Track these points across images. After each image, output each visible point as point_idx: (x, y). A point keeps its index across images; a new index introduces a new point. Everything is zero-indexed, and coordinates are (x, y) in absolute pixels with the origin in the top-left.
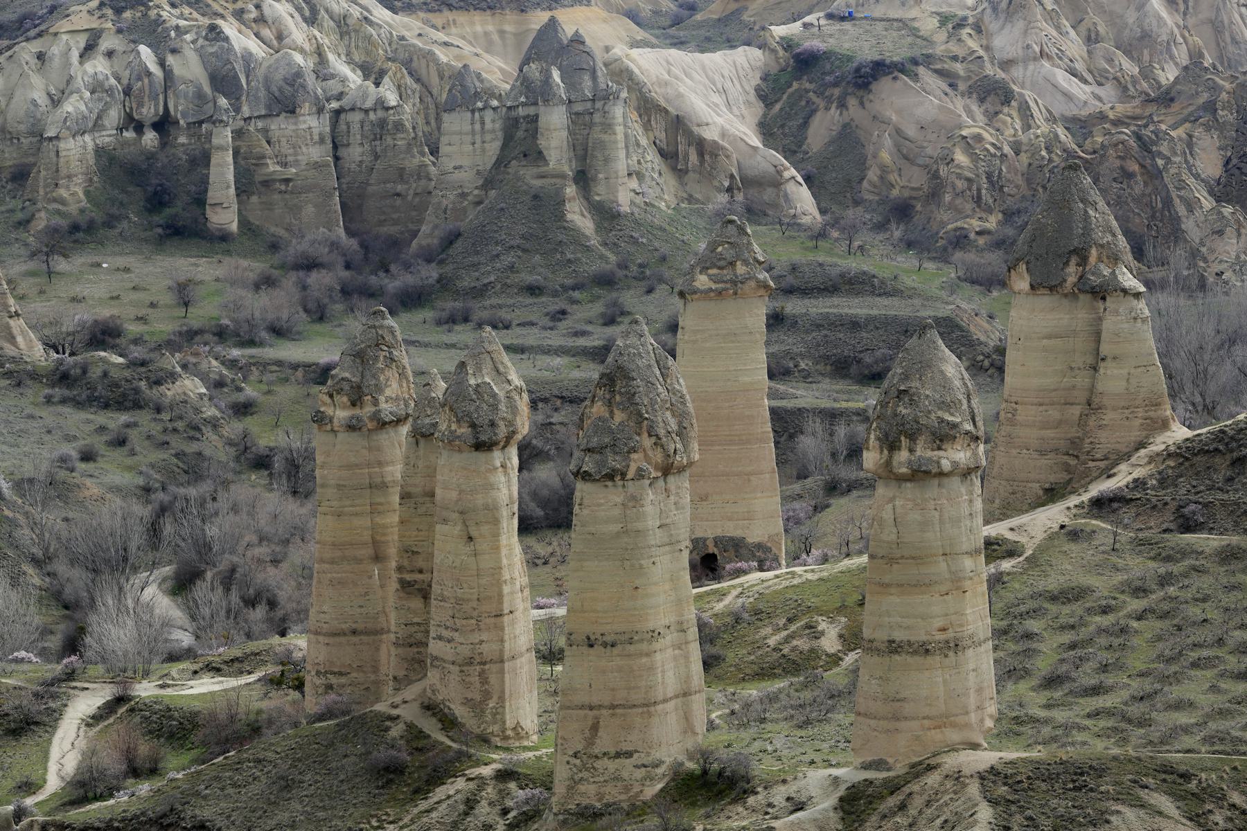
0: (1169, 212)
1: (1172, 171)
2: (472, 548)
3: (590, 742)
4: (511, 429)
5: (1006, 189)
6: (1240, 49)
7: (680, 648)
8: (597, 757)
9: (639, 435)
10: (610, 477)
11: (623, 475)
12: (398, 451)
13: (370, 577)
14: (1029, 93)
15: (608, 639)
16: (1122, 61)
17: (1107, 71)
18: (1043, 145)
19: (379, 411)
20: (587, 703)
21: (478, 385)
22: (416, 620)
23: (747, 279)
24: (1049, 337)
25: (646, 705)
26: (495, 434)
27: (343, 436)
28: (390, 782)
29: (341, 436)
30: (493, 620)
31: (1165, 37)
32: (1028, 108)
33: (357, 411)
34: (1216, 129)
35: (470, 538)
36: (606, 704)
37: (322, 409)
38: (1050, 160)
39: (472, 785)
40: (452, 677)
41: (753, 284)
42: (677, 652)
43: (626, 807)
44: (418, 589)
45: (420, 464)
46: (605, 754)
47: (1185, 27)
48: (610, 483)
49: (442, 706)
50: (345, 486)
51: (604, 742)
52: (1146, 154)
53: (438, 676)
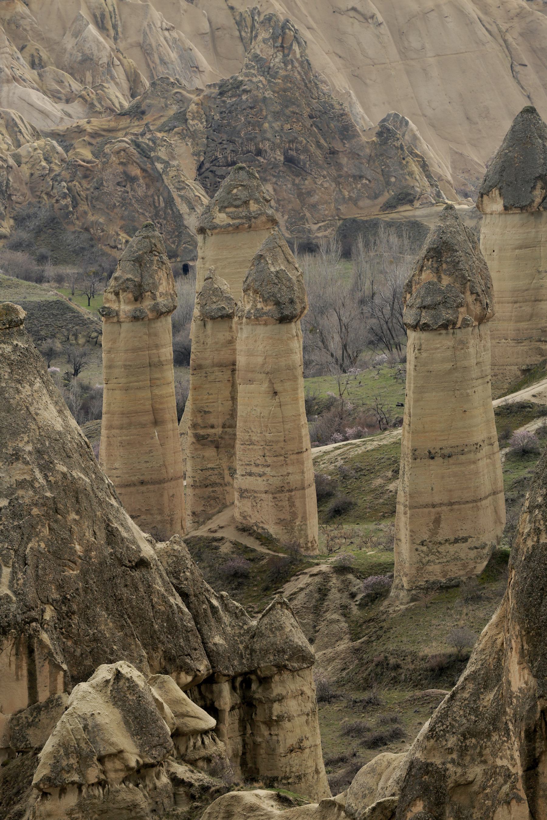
0: (172, 210)
1: (172, 174)
2: (277, 400)
3: (434, 532)
4: (303, 305)
5: (14, 198)
6: (168, 69)
7: (490, 458)
8: (440, 543)
9: (463, 293)
10: (445, 326)
11: (454, 324)
12: (168, 336)
13: (152, 438)
14: (14, 111)
15: (446, 452)
16: (71, 82)
17: (58, 92)
18: (42, 157)
19: (158, 304)
20: (430, 503)
21: (277, 272)
22: (210, 466)
23: (259, 214)
24: (520, 247)
25: (475, 501)
26: (295, 309)
27: (125, 326)
28: (240, 584)
29: (125, 326)
30: (295, 456)
31: (105, 60)
32: (16, 125)
33: (138, 305)
34: (189, 137)
35: (276, 393)
36: (446, 502)
37: (107, 305)
38: (51, 170)
39: (317, 579)
40: (264, 504)
41: (264, 218)
42: (488, 460)
43: (465, 580)
44: (211, 441)
45: (209, 341)
46: (446, 541)
47: (118, 51)
48: (444, 332)
49: (255, 528)
50: (131, 366)
51: (445, 532)
52: (146, 159)
53: (249, 504)
